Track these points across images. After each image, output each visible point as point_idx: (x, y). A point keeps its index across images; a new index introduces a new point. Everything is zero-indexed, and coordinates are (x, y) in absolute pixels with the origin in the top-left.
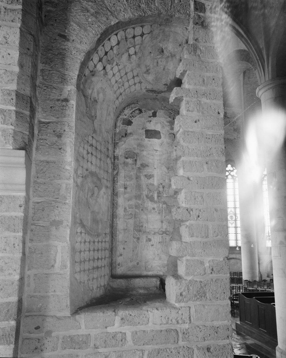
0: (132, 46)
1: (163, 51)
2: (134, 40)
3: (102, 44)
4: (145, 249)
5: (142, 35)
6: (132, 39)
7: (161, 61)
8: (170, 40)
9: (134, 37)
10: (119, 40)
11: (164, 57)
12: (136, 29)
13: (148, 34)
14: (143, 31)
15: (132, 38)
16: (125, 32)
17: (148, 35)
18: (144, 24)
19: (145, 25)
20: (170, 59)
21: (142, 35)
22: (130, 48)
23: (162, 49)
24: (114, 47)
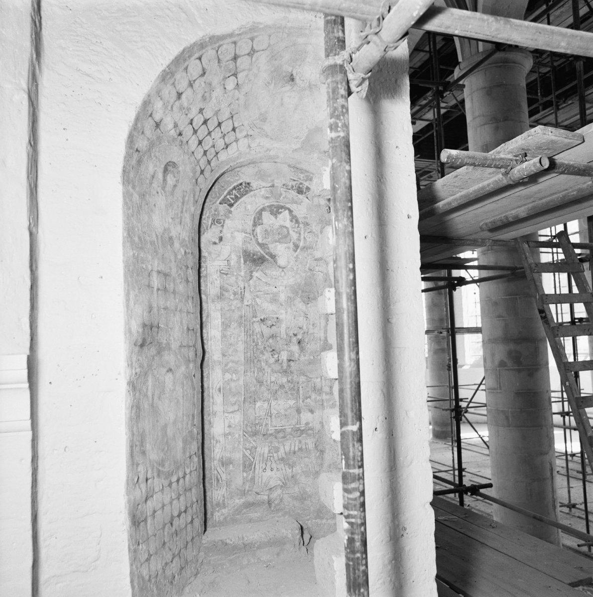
0: (231, 74)
1: (293, 80)
2: (236, 63)
3: (171, 81)
4: (267, 468)
5: (252, 52)
6: (231, 62)
7: (288, 96)
8: (307, 60)
9: (235, 58)
10: (205, 66)
11: (294, 89)
12: (239, 44)
13: (263, 50)
14: (254, 46)
15: (232, 60)
16: (217, 51)
17: (263, 52)
18: (255, 34)
19: (257, 36)
20: (307, 92)
21: (252, 52)
22: (226, 78)
23: (292, 75)
24: (195, 81)
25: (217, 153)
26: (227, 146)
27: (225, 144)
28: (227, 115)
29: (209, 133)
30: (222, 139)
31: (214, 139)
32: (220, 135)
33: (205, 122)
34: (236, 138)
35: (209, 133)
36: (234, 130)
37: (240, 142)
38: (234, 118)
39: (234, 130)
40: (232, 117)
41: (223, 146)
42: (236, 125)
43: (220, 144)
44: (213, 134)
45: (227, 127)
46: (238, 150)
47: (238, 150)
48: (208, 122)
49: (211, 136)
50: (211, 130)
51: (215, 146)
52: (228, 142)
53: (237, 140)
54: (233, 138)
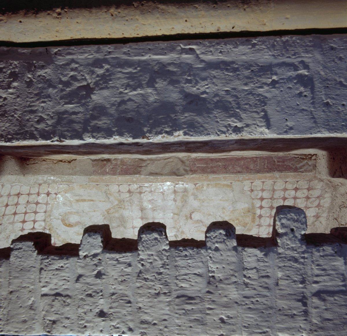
25: (28, 194)
26: (18, 195)
27: (19, 197)
28: (6, 218)
29: (26, 213)
30: (19, 202)
31: (25, 208)
32: (19, 207)
33: (24, 222)
34: (8, 198)
35: (26, 213)
36: (7, 205)
37: (7, 193)
38: (3, 213)
39: (7, 205)
40: (3, 215)
41: (22, 197)
42: (4, 208)
43: (22, 200)
44: (24, 211)
45: (10, 210)
46: (12, 186)
47: (12, 186)
48: (21, 221)
49: (26, 211)
50: (24, 215)
51: (26, 201)
52: (16, 197)
53: (9, 195)
54: (11, 199)
